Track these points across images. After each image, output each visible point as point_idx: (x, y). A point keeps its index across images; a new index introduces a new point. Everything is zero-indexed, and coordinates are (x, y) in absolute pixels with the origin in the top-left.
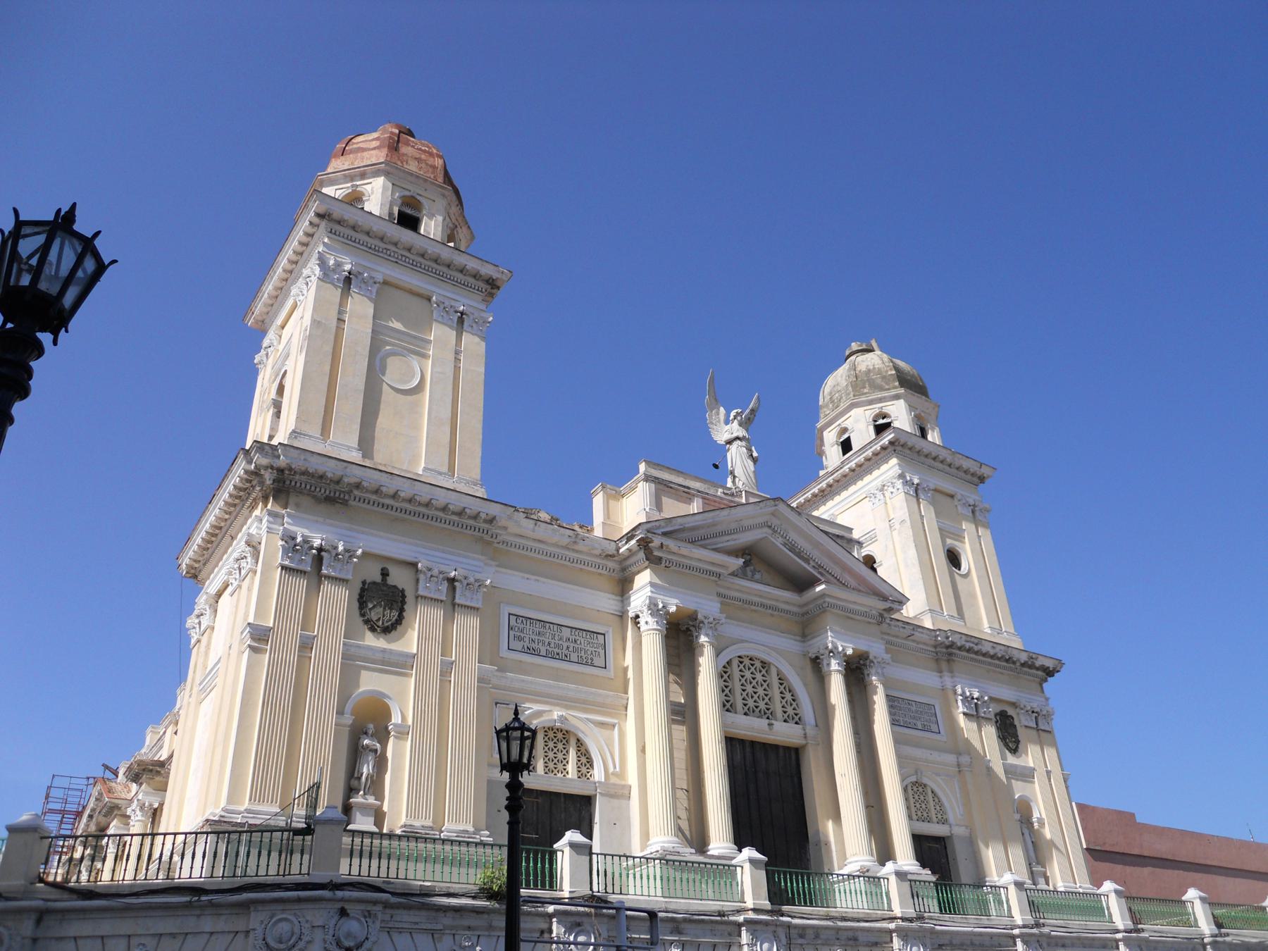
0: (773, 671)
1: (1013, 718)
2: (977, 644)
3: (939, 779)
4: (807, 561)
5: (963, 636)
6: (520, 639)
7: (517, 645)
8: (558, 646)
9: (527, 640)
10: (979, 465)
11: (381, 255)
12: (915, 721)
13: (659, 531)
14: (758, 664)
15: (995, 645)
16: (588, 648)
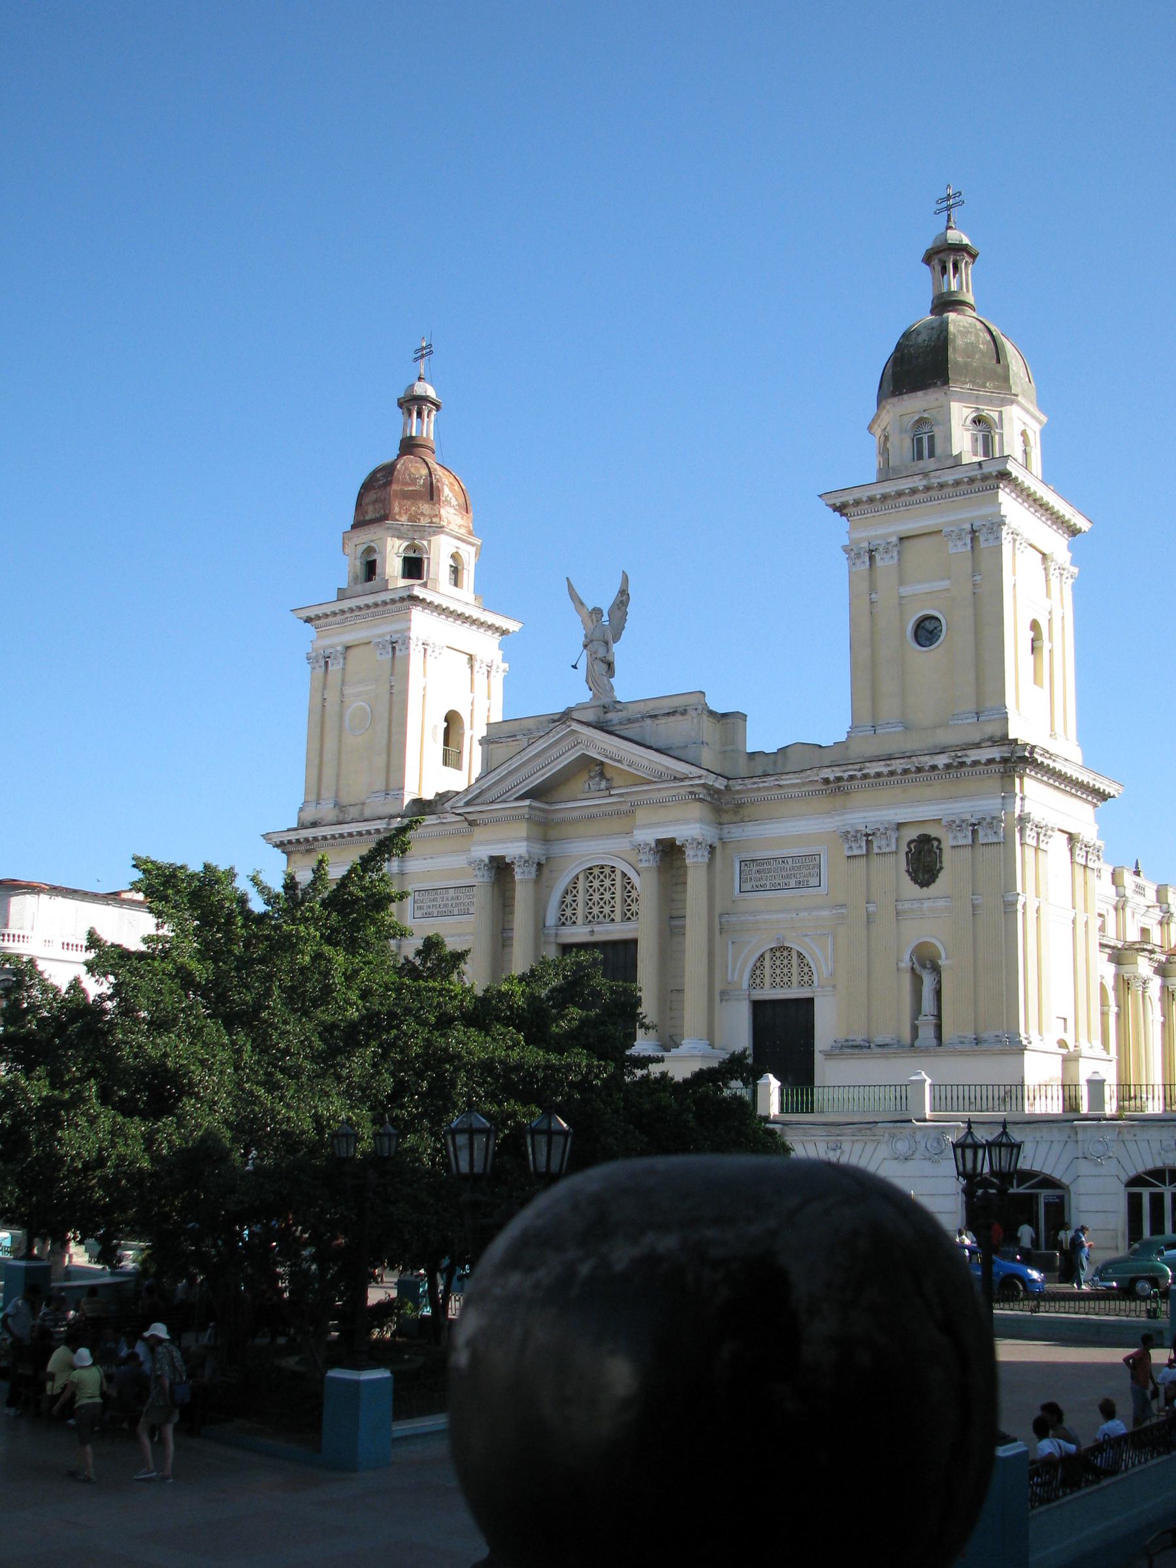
0: (618, 873)
1: (939, 841)
2: (860, 770)
3: (807, 939)
4: (619, 761)
5: (834, 769)
6: (420, 908)
7: (418, 914)
8: (446, 906)
9: (425, 908)
10: (977, 467)
11: (346, 624)
12: (787, 881)
13: (461, 804)
14: (607, 871)
15: (888, 762)
16: (466, 900)
